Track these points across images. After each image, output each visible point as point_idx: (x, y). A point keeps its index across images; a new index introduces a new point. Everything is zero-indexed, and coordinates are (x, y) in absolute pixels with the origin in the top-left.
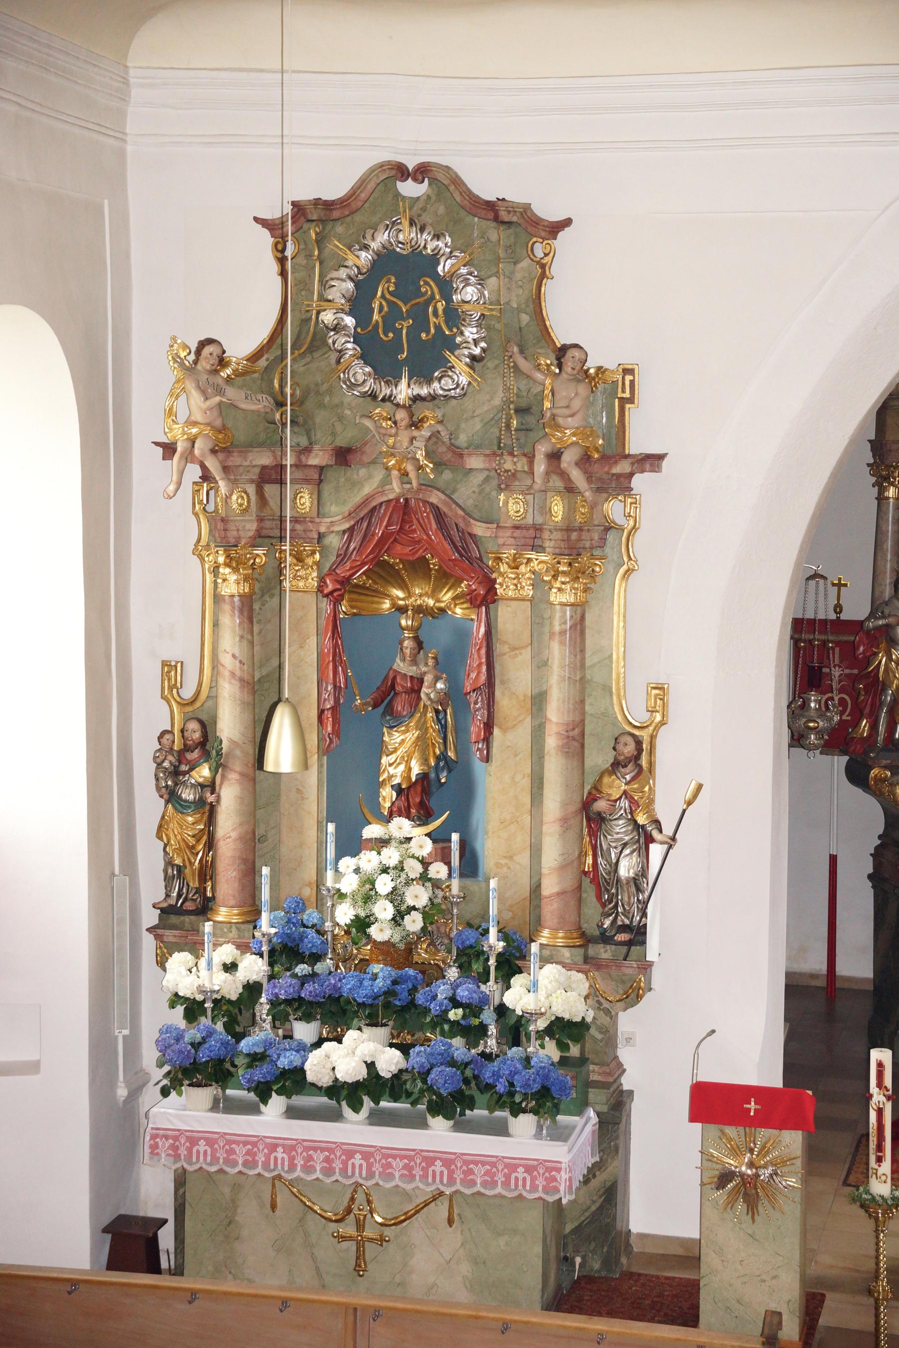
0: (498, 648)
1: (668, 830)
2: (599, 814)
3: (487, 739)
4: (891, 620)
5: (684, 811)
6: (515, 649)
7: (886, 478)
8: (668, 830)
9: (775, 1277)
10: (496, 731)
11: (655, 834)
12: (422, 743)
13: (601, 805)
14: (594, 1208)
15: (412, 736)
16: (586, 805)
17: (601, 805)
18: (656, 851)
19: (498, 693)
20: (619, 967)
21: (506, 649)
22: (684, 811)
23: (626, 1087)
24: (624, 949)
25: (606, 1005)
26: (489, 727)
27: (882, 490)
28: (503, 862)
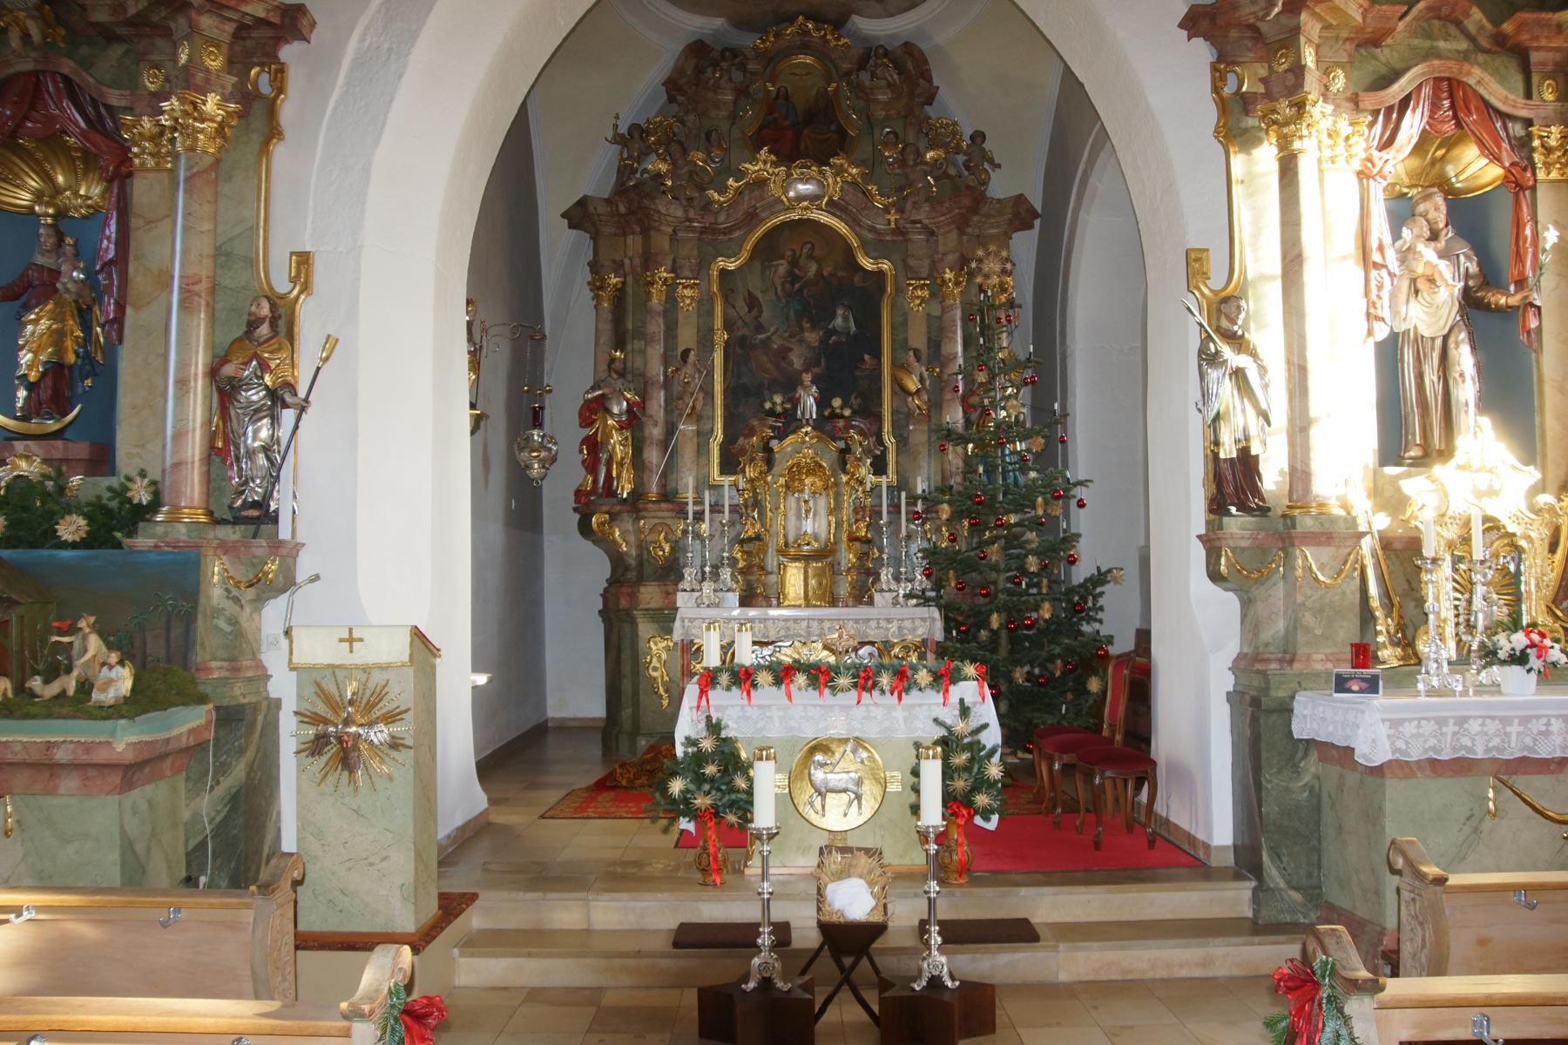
0: (135, 222)
1: (302, 394)
2: (231, 379)
3: (119, 320)
4: (606, 391)
5: (318, 369)
6: (149, 222)
7: (600, 288)
8: (302, 394)
9: (385, 858)
10: (129, 310)
11: (288, 398)
12: (57, 338)
13: (228, 370)
14: (218, 819)
15: (44, 324)
16: (213, 373)
17: (228, 370)
18: (288, 416)
19: (131, 270)
20: (247, 546)
21: (141, 222)
22: (318, 369)
23: (273, 695)
24: (252, 528)
25: (235, 592)
26: (121, 308)
27: (596, 297)
28: (135, 451)
